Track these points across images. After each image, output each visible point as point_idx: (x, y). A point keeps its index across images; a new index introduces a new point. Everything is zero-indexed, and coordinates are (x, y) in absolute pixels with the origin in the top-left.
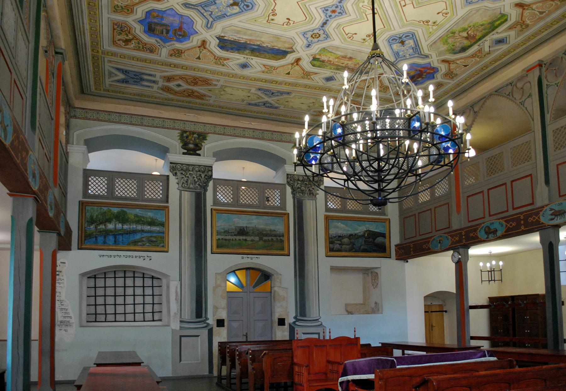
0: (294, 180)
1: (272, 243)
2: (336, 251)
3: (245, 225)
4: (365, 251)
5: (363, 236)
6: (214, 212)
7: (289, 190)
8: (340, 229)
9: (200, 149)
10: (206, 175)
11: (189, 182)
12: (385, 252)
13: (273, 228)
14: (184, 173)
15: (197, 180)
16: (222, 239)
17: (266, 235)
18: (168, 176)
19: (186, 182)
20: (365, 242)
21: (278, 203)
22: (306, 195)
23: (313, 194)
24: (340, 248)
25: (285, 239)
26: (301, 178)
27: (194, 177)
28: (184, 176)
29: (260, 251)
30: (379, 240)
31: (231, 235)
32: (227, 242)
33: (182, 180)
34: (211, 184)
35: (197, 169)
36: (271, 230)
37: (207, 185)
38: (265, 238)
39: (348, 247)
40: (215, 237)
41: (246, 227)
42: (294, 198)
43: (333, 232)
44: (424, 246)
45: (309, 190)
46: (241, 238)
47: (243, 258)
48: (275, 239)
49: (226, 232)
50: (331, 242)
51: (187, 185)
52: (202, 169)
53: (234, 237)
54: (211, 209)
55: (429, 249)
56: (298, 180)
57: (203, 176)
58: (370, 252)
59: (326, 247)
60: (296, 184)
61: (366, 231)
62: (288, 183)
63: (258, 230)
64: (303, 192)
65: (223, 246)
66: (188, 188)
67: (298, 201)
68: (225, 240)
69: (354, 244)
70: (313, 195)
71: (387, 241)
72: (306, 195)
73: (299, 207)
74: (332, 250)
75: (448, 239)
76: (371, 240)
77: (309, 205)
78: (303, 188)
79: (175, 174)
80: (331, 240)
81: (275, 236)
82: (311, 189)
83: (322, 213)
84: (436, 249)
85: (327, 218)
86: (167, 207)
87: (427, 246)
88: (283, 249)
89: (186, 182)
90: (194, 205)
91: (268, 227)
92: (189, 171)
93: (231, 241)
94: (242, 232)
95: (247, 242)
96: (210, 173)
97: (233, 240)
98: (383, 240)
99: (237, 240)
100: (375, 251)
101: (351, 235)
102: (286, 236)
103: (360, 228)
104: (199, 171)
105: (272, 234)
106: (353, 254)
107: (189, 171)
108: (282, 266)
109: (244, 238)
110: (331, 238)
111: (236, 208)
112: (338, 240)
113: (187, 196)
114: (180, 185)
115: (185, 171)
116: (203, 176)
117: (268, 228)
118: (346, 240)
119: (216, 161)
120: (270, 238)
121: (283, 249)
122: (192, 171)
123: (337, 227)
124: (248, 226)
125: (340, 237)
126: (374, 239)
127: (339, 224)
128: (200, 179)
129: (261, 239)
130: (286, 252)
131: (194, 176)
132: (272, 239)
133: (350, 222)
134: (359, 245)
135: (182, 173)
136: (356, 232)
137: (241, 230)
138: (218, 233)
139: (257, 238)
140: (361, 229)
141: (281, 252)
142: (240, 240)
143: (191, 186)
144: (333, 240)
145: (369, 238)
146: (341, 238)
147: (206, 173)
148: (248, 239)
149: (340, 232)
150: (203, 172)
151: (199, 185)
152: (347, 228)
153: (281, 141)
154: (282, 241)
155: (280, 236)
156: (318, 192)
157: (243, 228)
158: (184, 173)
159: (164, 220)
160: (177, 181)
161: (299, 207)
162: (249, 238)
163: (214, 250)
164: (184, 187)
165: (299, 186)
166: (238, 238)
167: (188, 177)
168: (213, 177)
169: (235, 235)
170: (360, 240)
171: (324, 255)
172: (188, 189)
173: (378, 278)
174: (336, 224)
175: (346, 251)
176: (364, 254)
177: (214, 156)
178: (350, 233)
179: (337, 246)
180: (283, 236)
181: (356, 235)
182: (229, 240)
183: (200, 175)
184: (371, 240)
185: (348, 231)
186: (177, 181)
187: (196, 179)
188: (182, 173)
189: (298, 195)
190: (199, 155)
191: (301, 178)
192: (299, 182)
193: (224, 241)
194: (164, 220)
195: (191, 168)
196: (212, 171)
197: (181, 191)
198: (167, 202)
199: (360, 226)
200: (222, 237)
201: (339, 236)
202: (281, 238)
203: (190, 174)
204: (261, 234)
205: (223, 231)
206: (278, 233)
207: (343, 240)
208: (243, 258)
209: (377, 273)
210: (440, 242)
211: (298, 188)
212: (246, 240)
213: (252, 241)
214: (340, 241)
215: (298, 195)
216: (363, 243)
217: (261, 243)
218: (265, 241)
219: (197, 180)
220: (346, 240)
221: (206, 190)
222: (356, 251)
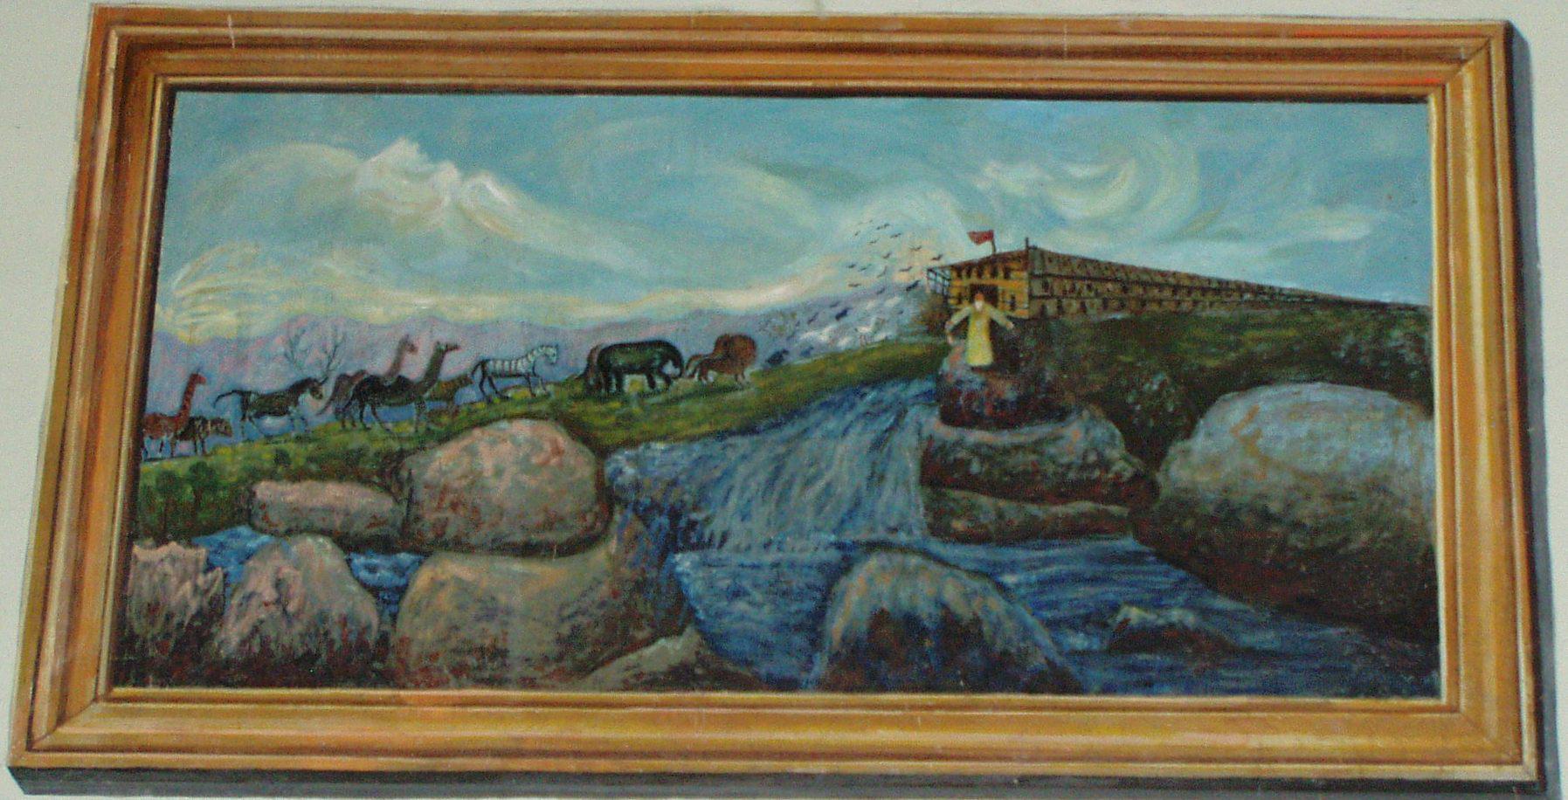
2: (264, 668)
12: (1417, 675)
20: (938, 472)
30: (1268, 441)
39: (530, 591)
43: (228, 305)
50: (157, 514)
58: (1059, 680)
61: (980, 278)
69: (681, 530)
80: (171, 459)
101: (614, 379)
103: (853, 222)
110: (188, 427)
112: (346, 468)
123: (337, 221)
125: (390, 405)
126: (1153, 438)
134: (814, 548)
140: (837, 239)
144: (229, 457)
145: (1041, 406)
146: (394, 425)
149: (385, 309)
152: (543, 231)
170: (839, 450)
174: (331, 158)
178: (599, 313)
179: (297, 575)
181: (732, 349)
184: (1080, 437)
185: (571, 275)
199: (838, 184)
201: (368, 391)
207: (443, 463)
214: (389, 472)
216: (901, 502)
220: (507, 461)
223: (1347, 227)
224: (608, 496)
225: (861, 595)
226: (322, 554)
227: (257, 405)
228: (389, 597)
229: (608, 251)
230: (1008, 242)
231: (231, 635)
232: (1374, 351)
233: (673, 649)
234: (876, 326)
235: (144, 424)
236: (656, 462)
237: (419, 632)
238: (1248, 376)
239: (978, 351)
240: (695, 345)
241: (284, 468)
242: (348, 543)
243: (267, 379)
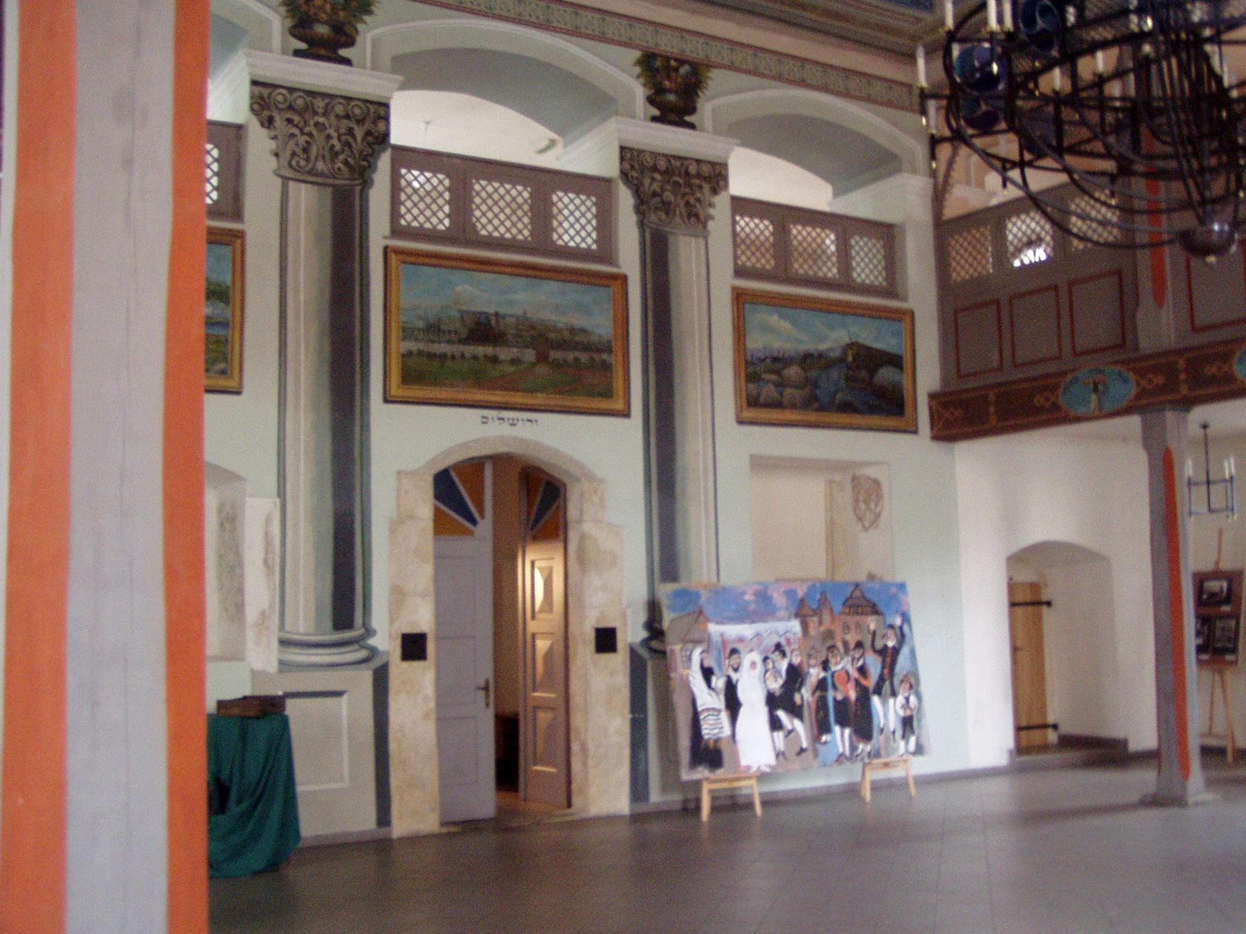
0: (643, 169)
1: (573, 372)
2: (767, 405)
3: (491, 310)
4: (847, 408)
5: (842, 360)
6: (393, 258)
7: (625, 199)
8: (780, 334)
9: (350, 43)
10: (368, 133)
11: (314, 151)
13: (579, 321)
14: (297, 119)
15: (338, 147)
16: (420, 353)
17: (561, 345)
18: (239, 128)
19: (305, 150)
20: (847, 379)
21: (589, 241)
22: (678, 220)
23: (697, 216)
24: (775, 395)
25: (615, 359)
26: (662, 164)
27: (329, 137)
28: (296, 131)
29: (540, 399)
30: (886, 375)
31: (448, 342)
32: (436, 363)
33: (292, 143)
34: (384, 161)
35: (339, 109)
36: (572, 330)
37: (372, 167)
38: (555, 355)
39: (798, 393)
40: (400, 346)
41: (497, 315)
42: (642, 225)
43: (757, 342)
44: (1038, 400)
45: (687, 203)
46: (480, 350)
47: (485, 420)
48: (584, 358)
49: (434, 329)
50: (753, 378)
51: (308, 160)
52: (357, 111)
53: (457, 349)
54: (386, 249)
55: (1056, 407)
56: (655, 169)
57: (359, 132)
59: (737, 391)
60: (647, 182)
62: (624, 174)
63: (533, 327)
64: (667, 207)
65: (423, 378)
66: (310, 173)
67: (653, 236)
68: (431, 356)
69: (815, 385)
70: (697, 219)
71: (906, 382)
72: (678, 220)
73: (657, 257)
74: (753, 402)
75: (1126, 381)
76: (863, 374)
77: (686, 250)
78: (668, 196)
79: (268, 123)
80: (750, 370)
81: (587, 348)
82: (692, 201)
83: (724, 283)
84: (1082, 410)
85: (740, 298)
86: (241, 235)
87: (1047, 399)
88: (608, 394)
89: (305, 150)
90: (327, 231)
91: (565, 320)
92: (315, 113)
93: (449, 363)
94: (483, 330)
95: (500, 367)
96: (381, 126)
97: (453, 357)
98: (897, 378)
99: (466, 357)
100: (872, 410)
101: (807, 360)
102: (620, 354)
104: (347, 117)
105: (574, 340)
106: (812, 417)
107: (315, 113)
108: (598, 451)
109: (489, 350)
110: (752, 364)
111: (460, 249)
113: (306, 198)
114: (284, 162)
115: (300, 113)
116: (359, 132)
117: (562, 321)
118: (793, 372)
119: (403, 87)
120: (570, 356)
121: (608, 394)
122: (325, 114)
123: (768, 329)
124: (502, 311)
125: (779, 362)
126: (872, 373)
127: (775, 319)
128: (347, 144)
129: (542, 358)
130: (619, 406)
131: (331, 132)
132: (577, 360)
133: (804, 315)
135: (289, 121)
136: (823, 347)
137: (478, 324)
138: (407, 333)
139: (529, 355)
140: (833, 337)
141: (604, 404)
142: (475, 358)
143: (321, 166)
145: (858, 367)
146: (778, 365)
147: (368, 125)
148: (502, 357)
150: (360, 122)
151: (346, 163)
153: (602, 38)
154: (606, 367)
155: (599, 351)
156: (711, 211)
157: (488, 316)
158: (297, 119)
159: (229, 282)
160: (273, 145)
161: (657, 257)
162: (504, 354)
163: (395, 391)
164: (297, 166)
165: (656, 187)
166: (469, 350)
167: (310, 135)
168: (394, 139)
169: (461, 341)
170: (836, 374)
171: (731, 416)
172: (309, 175)
173: (879, 497)
175: (793, 407)
176: (844, 418)
177: (395, 70)
179: (769, 391)
180: (609, 350)
181: (820, 356)
182: (442, 357)
183: (350, 132)
185: (802, 342)
186: (273, 145)
187: (335, 142)
188: (289, 121)
189: (653, 218)
190: (347, 62)
191: (662, 164)
192: (657, 176)
193: (425, 360)
194: (229, 282)
195: (320, 104)
196: (386, 119)
197: (285, 179)
198: (238, 215)
199: (832, 328)
200: (421, 346)
201: (775, 359)
202: (605, 356)
203: (317, 124)
204: (543, 340)
205: (421, 324)
206: (594, 339)
208: (485, 420)
209: (877, 483)
210: (1096, 390)
211: (655, 194)
212: (495, 360)
213: (514, 362)
214: (778, 373)
215: (653, 218)
217: (542, 369)
218: (557, 365)
219: (338, 147)
220: (793, 372)
221: (366, 183)
222: (822, 409)
223: (893, 341)
224: (807, 379)
225: (839, 396)
226: (772, 388)
227: (762, 361)
228: (781, 394)
229: (805, 338)
230: (854, 340)
231: (762, 399)
232: (895, 361)
233: (815, 405)
234: (837, 353)
235: (747, 363)
236: (813, 374)
237: (785, 401)
238: (882, 365)
239: (850, 358)
240: (816, 354)
241: (765, 372)
242: (777, 385)
243: (761, 356)
